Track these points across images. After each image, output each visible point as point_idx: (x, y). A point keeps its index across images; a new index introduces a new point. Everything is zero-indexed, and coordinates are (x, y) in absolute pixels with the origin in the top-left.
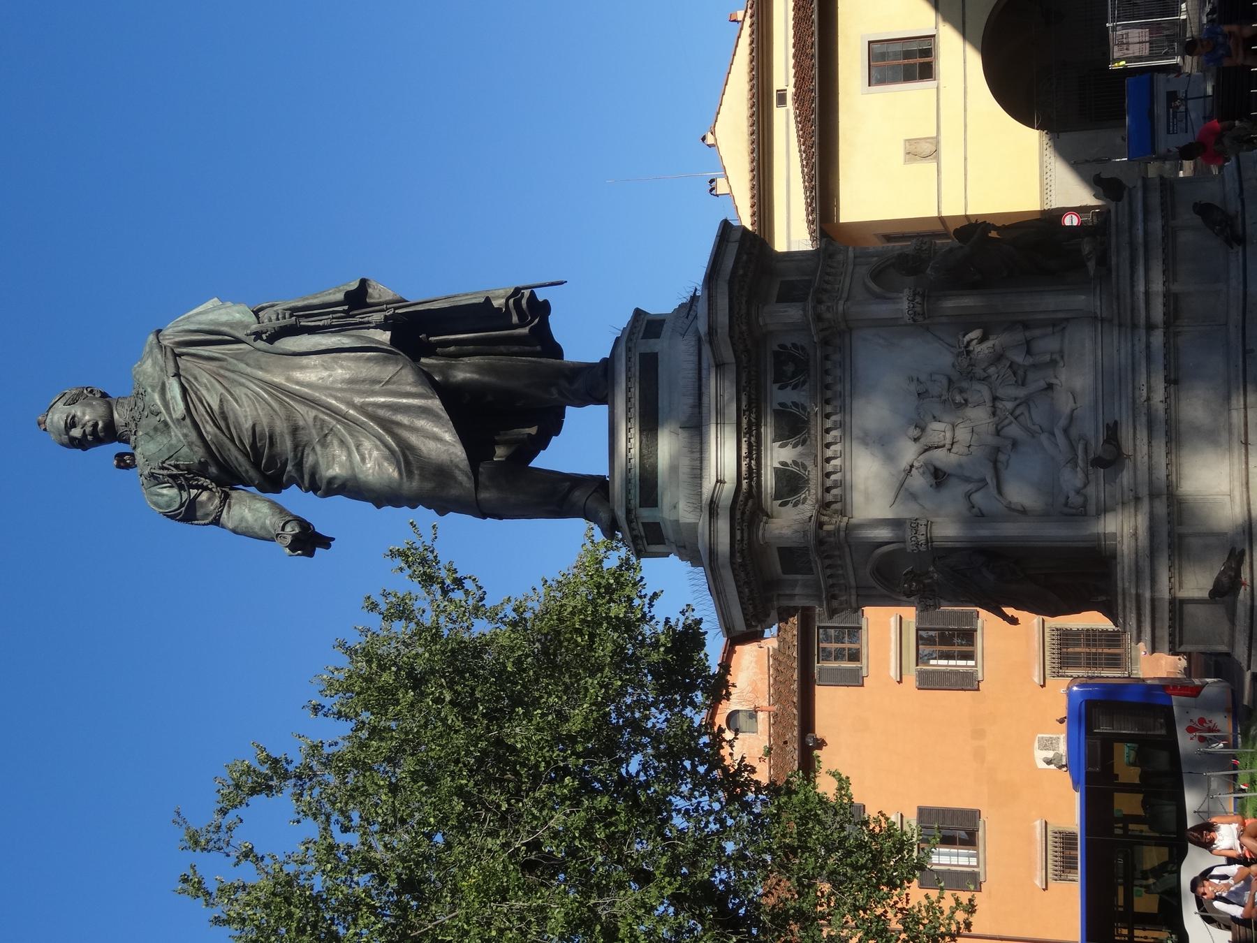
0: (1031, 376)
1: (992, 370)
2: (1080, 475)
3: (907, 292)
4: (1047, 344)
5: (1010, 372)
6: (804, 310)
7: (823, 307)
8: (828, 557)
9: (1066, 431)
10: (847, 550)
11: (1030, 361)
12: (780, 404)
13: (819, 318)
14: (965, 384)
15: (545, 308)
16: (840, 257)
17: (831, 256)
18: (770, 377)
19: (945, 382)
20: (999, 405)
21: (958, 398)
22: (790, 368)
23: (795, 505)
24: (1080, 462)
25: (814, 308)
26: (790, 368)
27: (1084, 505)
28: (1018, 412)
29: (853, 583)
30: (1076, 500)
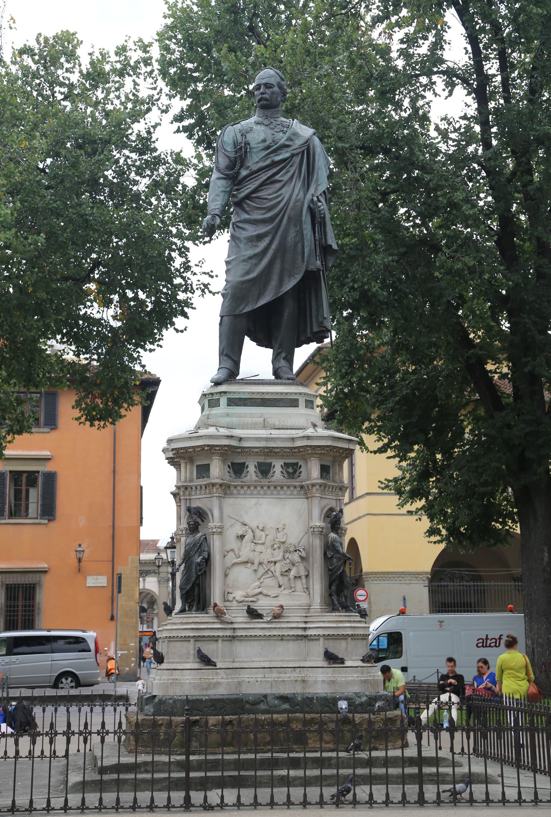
0: (286, 579)
1: (288, 561)
2: (242, 599)
4: (299, 585)
5: (287, 569)
6: (317, 479)
7: (318, 487)
8: (206, 487)
9: (261, 593)
10: (209, 496)
13: (313, 485)
14: (282, 550)
16: (340, 493)
17: (341, 489)
19: (283, 540)
20: (272, 564)
21: (276, 546)
22: (291, 470)
23: (229, 472)
24: (247, 599)
25: (318, 484)
26: (291, 470)
28: (269, 572)
29: (192, 497)
30: (230, 597)
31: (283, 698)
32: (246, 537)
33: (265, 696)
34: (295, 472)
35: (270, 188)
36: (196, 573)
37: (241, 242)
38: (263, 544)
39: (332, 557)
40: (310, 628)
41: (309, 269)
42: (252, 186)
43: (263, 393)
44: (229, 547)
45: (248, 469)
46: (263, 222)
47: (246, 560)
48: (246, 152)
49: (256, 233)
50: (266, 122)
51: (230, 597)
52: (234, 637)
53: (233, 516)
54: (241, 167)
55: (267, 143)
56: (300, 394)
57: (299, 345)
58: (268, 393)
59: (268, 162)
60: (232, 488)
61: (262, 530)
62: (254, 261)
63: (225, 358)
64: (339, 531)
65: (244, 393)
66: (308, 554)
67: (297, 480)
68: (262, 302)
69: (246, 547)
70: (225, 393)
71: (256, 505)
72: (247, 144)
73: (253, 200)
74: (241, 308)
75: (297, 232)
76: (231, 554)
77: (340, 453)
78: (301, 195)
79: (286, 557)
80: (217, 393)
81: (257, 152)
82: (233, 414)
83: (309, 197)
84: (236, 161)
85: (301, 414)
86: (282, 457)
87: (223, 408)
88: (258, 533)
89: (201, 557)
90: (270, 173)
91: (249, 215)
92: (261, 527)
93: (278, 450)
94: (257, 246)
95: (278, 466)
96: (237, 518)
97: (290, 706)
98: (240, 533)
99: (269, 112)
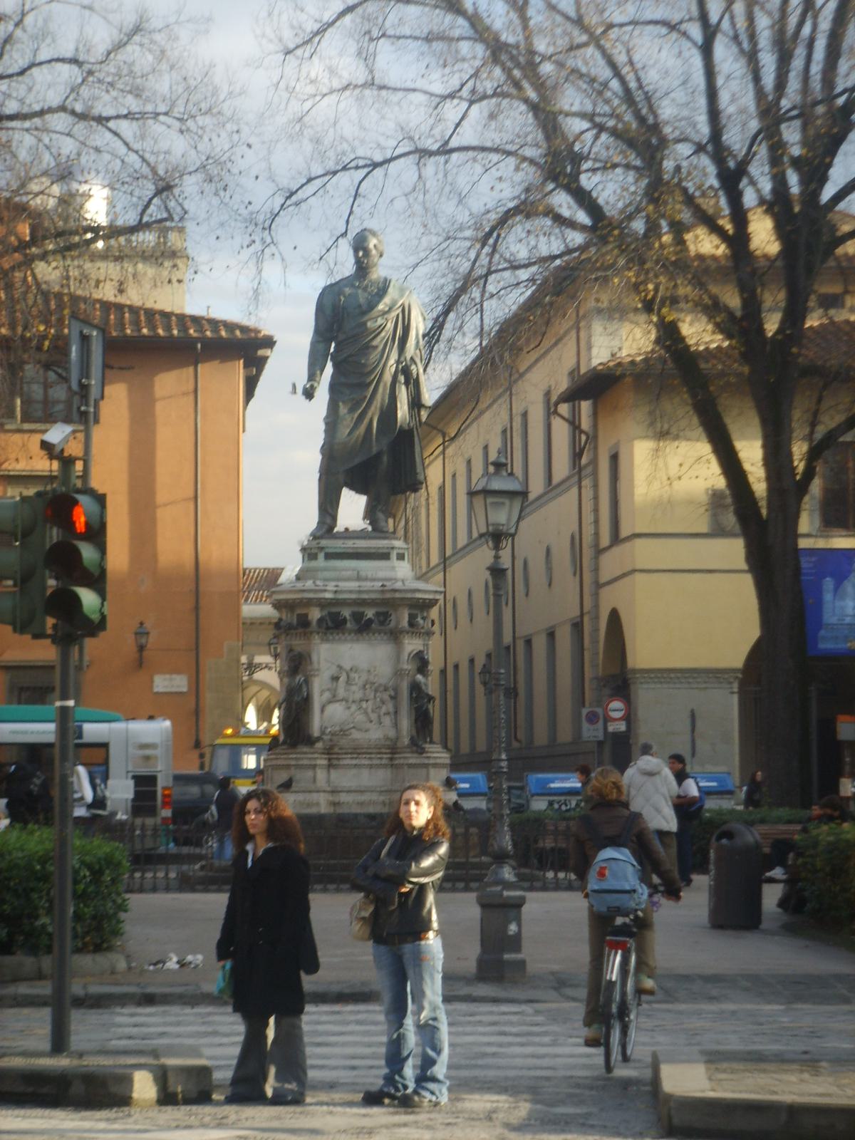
26: (382, 618)
33: (356, 815)
66: (396, 694)
87: (321, 562)
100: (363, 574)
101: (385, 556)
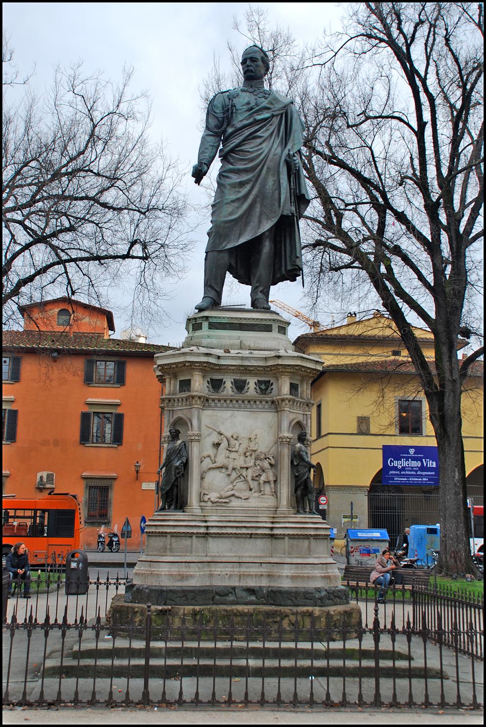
0: (256, 483)
1: (258, 467)
3: (291, 435)
4: (267, 489)
5: (257, 474)
6: (286, 394)
7: (287, 402)
8: (186, 399)
9: (233, 495)
10: (189, 407)
11: (262, 482)
12: (249, 382)
13: (283, 400)
14: (253, 456)
15: (294, 280)
16: (307, 409)
17: (307, 405)
18: (260, 379)
19: (255, 449)
20: (244, 470)
21: (248, 454)
22: (263, 387)
23: (208, 387)
24: (220, 500)
25: (287, 399)
26: (263, 387)
27: (203, 501)
28: (241, 477)
29: (175, 409)
30: (206, 498)
31: (251, 591)
32: (222, 445)
33: (234, 588)
34: (267, 389)
35: (253, 143)
36: (175, 475)
37: (225, 187)
38: (236, 452)
39: (297, 465)
40: (276, 528)
41: (284, 214)
42: (236, 141)
43: (241, 319)
44: (205, 454)
45: (225, 385)
46: (246, 171)
47: (221, 465)
48: (232, 113)
49: (238, 180)
50: (251, 90)
51: (206, 498)
52: (207, 534)
53: (211, 427)
54: (228, 125)
55: (251, 105)
56: (274, 320)
57: (274, 283)
58: (245, 319)
59: (251, 120)
60: (210, 401)
61: (236, 439)
62: (236, 204)
63: (209, 288)
64: (305, 442)
65: (224, 318)
66: (276, 462)
67: (269, 396)
68: (242, 241)
69: (221, 454)
70: (207, 317)
71: (231, 416)
72: (233, 106)
73: (237, 153)
74: (224, 245)
75: (274, 181)
76: (207, 460)
77: (307, 372)
78: (279, 150)
79: (257, 464)
80: (199, 318)
81: (242, 113)
82: (213, 336)
83: (286, 152)
84: (223, 121)
85: (275, 339)
86: (256, 375)
88: (232, 441)
89: (180, 461)
90: (252, 130)
91: (233, 165)
92: (235, 437)
93: (252, 368)
94: (239, 192)
95: (252, 382)
96: (214, 428)
97: (257, 598)
98: (216, 441)
99: (254, 83)
100: (247, 343)
101: (267, 328)
